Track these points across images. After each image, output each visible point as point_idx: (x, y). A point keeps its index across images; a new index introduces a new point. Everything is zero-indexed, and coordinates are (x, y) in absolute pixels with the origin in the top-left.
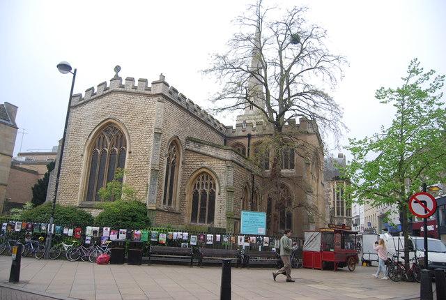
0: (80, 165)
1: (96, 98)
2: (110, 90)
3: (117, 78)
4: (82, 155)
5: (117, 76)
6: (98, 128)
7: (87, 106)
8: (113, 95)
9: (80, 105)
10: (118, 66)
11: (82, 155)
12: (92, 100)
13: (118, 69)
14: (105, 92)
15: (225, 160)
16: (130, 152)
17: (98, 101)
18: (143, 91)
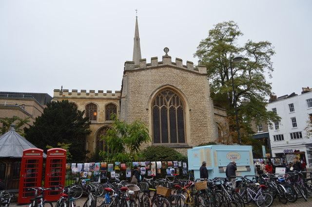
0: (147, 118)
1: (197, 73)
2: (164, 64)
3: (167, 57)
4: (147, 109)
5: (167, 54)
6: (158, 90)
7: (143, 72)
8: (167, 68)
9: (137, 71)
10: (166, 48)
11: (147, 109)
12: (148, 69)
13: (166, 50)
14: (159, 65)
15: (223, 117)
16: (190, 110)
17: (154, 71)
18: (193, 71)
